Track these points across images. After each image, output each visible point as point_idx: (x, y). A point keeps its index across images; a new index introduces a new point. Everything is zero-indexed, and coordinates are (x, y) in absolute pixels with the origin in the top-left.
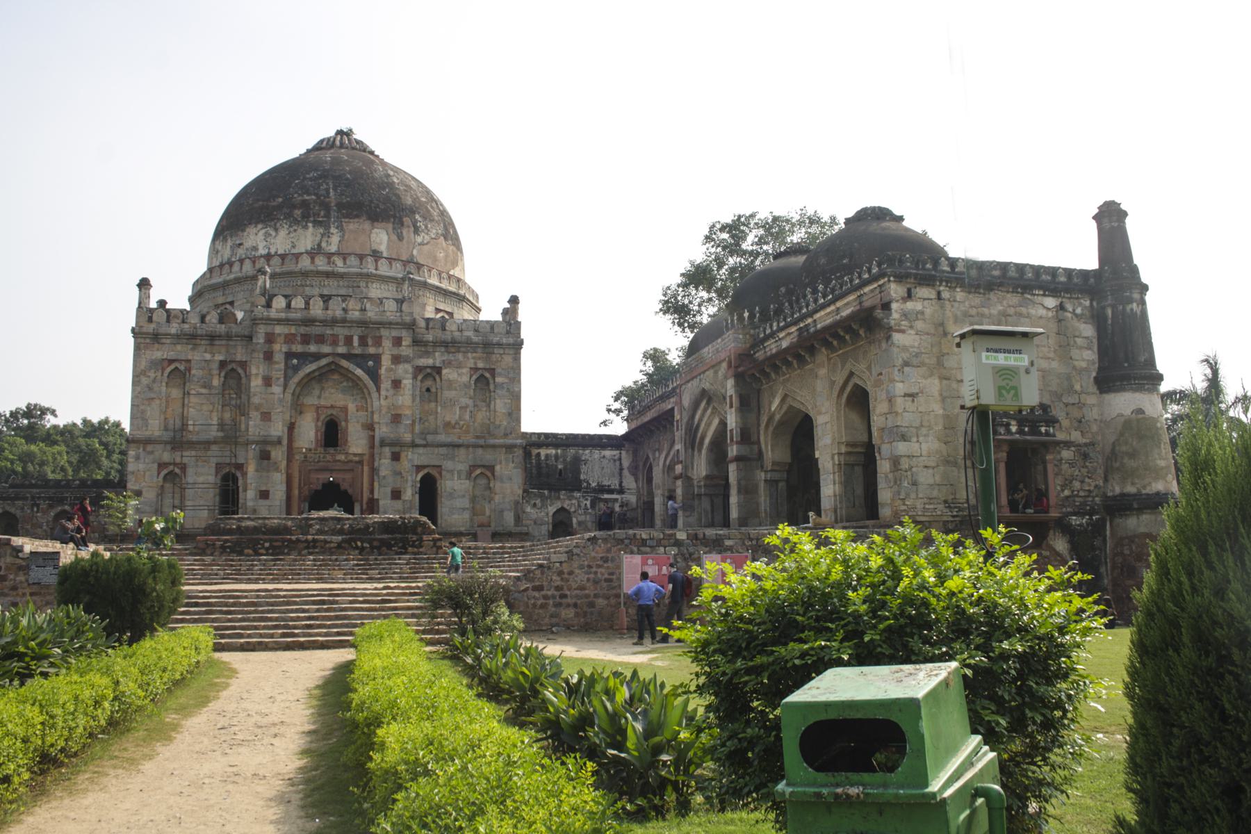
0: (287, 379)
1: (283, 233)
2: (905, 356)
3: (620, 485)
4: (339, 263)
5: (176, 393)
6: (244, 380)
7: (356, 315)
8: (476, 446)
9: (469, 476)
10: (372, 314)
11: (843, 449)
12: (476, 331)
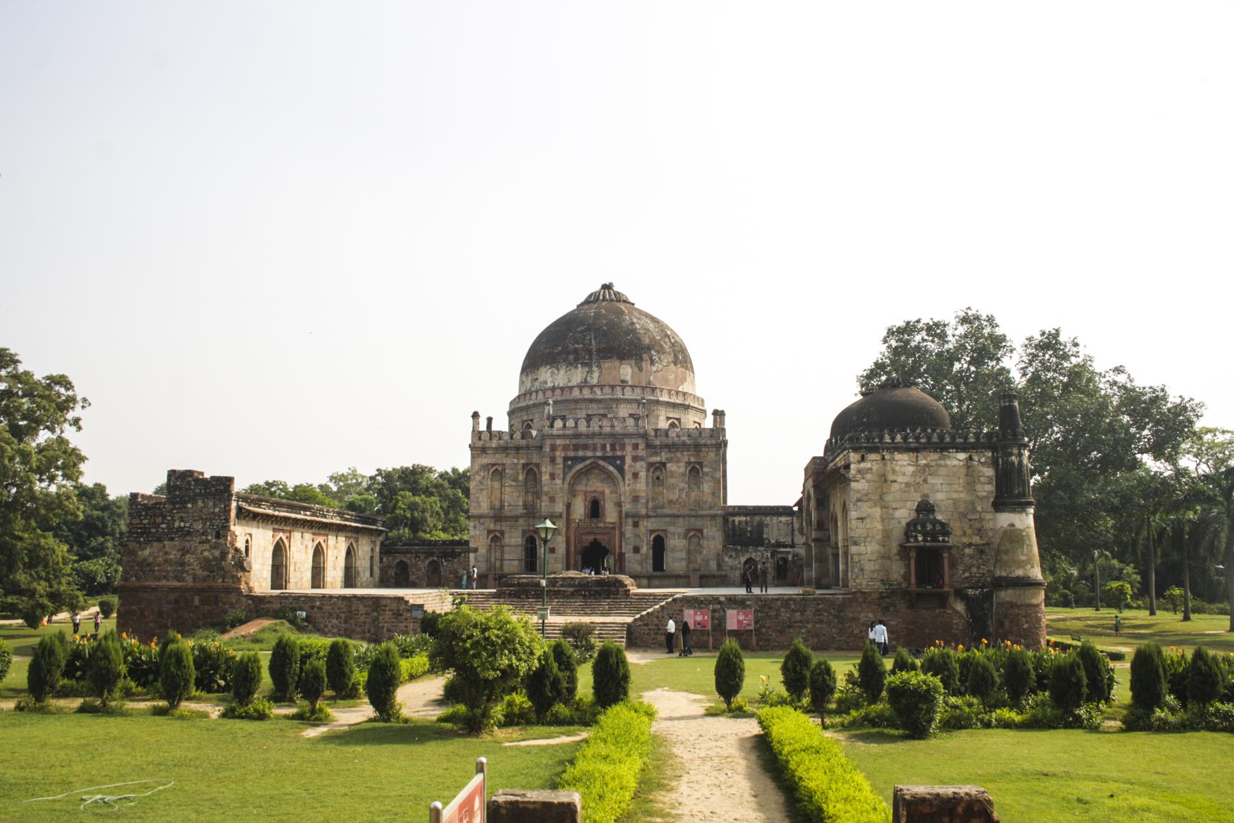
0: (565, 474)
1: (562, 372)
2: (858, 495)
4: (598, 391)
5: (497, 485)
7: (607, 430)
9: (685, 536)
10: (618, 428)
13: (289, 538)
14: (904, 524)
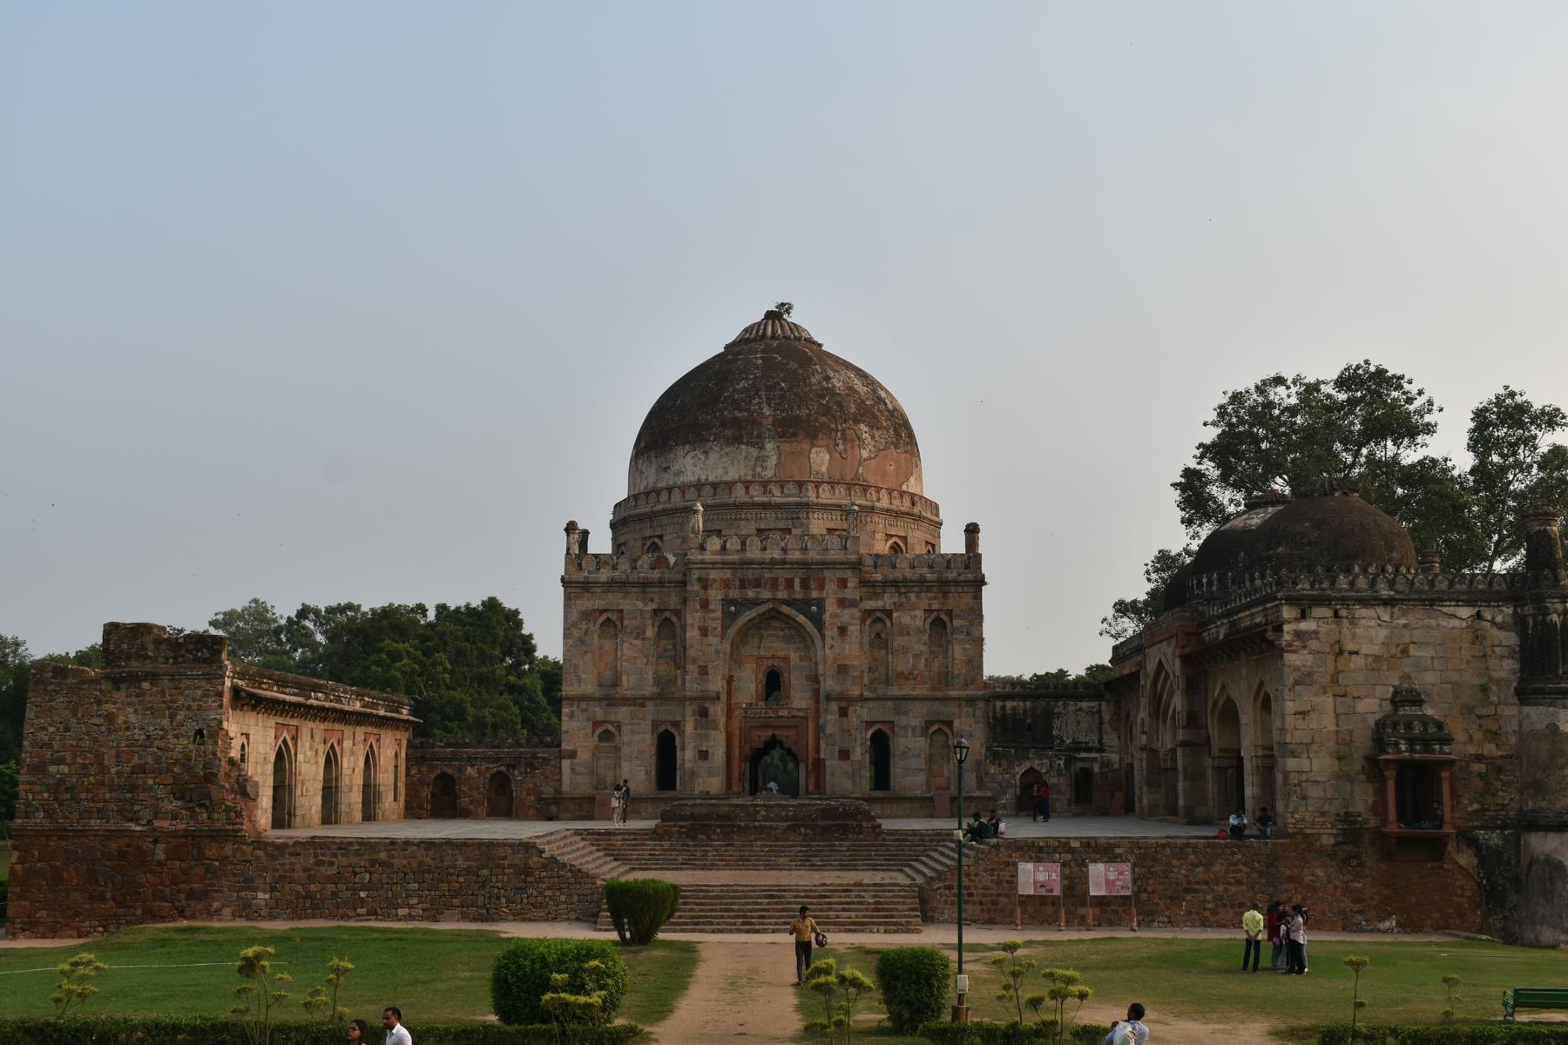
0: (725, 627)
1: (713, 457)
2: (1297, 675)
3: (1100, 741)
4: (777, 492)
5: (608, 645)
6: (678, 631)
7: (796, 555)
8: (934, 699)
9: (924, 731)
10: (814, 555)
11: (1261, 753)
12: (931, 567)
13: (295, 739)
14: (1372, 724)
